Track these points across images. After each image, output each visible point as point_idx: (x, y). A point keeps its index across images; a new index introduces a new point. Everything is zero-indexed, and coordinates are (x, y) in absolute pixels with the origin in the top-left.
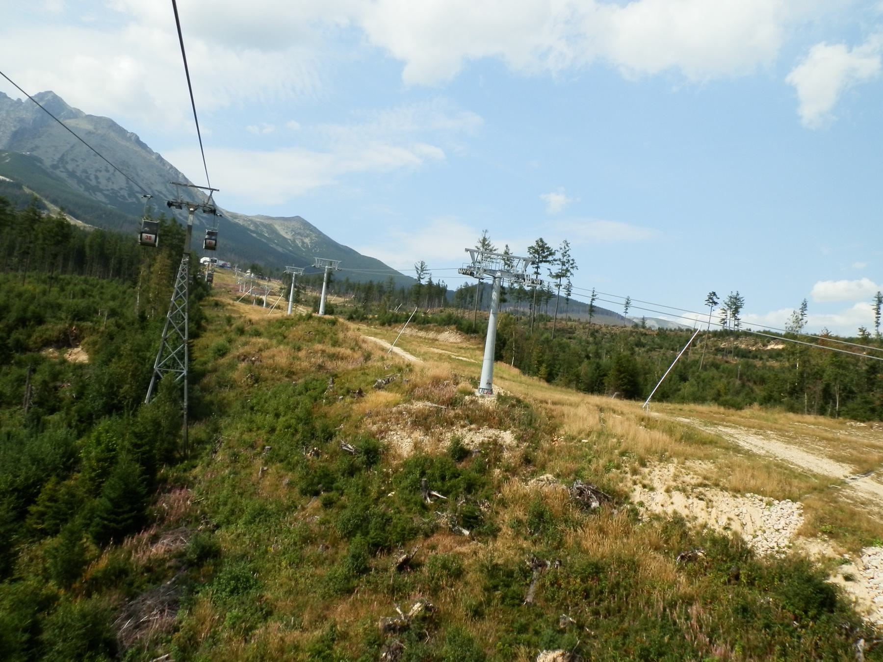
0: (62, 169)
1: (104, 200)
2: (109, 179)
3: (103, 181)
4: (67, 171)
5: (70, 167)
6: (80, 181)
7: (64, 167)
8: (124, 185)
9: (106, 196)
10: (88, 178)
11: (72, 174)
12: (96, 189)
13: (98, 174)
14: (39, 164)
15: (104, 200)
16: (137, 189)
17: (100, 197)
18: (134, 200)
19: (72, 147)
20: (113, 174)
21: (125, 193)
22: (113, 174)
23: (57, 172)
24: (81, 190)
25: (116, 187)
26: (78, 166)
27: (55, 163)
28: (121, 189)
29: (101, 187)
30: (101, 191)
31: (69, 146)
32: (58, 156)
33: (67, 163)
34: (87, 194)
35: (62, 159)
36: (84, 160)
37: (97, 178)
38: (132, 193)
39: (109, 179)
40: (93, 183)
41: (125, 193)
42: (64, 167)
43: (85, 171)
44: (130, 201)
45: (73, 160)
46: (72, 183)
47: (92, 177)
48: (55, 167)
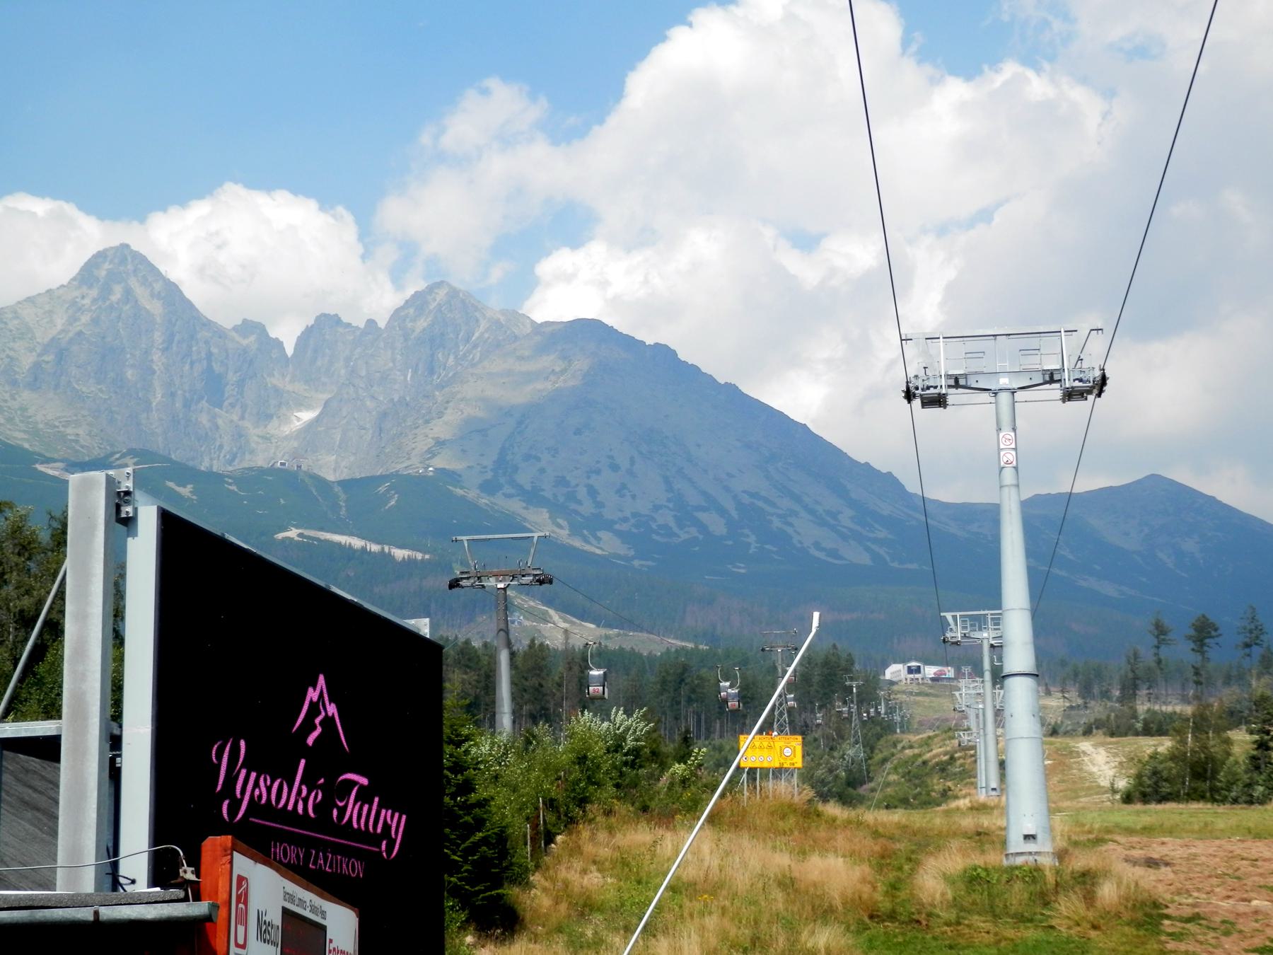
0: (508, 490)
2: (621, 490)
10: (571, 496)
14: (459, 492)
18: (694, 531)
19: (520, 423)
20: (630, 473)
22: (630, 473)
26: (542, 471)
27: (489, 475)
28: (657, 508)
33: (516, 469)
34: (577, 543)
35: (502, 463)
37: (592, 492)
39: (621, 490)
40: (587, 508)
43: (561, 481)
44: (684, 536)
45: (527, 457)
47: (582, 493)
48: (489, 487)
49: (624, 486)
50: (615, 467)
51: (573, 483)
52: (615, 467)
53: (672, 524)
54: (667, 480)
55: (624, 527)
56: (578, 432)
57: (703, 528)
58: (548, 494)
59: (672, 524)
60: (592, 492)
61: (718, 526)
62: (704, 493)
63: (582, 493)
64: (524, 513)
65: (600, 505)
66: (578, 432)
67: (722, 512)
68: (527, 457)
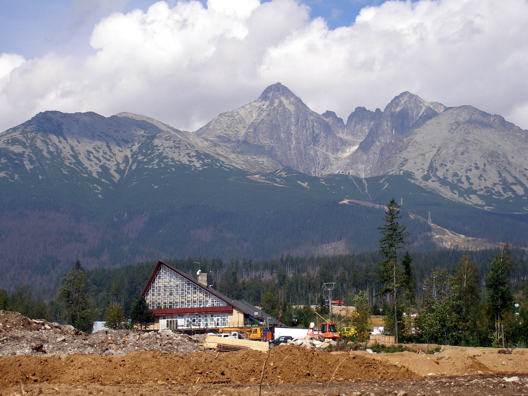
0: (433, 179)
1: (480, 202)
2: (480, 177)
3: (474, 180)
4: (439, 179)
5: (440, 174)
6: (453, 187)
7: (435, 175)
8: (497, 179)
9: (481, 197)
10: (459, 181)
11: (444, 182)
12: (470, 191)
13: (469, 174)
14: (413, 181)
15: (480, 202)
16: (510, 180)
17: (475, 200)
19: (438, 151)
21: (499, 188)
22: (484, 170)
23: (430, 183)
24: (456, 197)
25: (489, 184)
26: (447, 170)
27: (426, 173)
28: (495, 184)
29: (474, 188)
30: (475, 192)
31: (435, 151)
32: (427, 164)
33: (437, 170)
34: (461, 200)
35: (431, 167)
36: (452, 162)
37: (468, 178)
38: (507, 187)
39: (480, 177)
40: (466, 185)
41: (499, 188)
42: (435, 175)
43: (455, 175)
44: (506, 196)
45: (441, 165)
46: (446, 193)
47: (464, 179)
48: (426, 178)
49: (481, 176)
50: (477, 168)
51: (460, 175)
52: (477, 168)
53: (501, 191)
54: (499, 172)
55: (481, 193)
56: (462, 154)
57: (514, 192)
58: (450, 180)
59: (501, 191)
60: (468, 178)
61: (520, 191)
62: (515, 178)
63: (464, 179)
64: (440, 188)
65: (471, 184)
66: (462, 154)
67: (522, 185)
68: (441, 165)
